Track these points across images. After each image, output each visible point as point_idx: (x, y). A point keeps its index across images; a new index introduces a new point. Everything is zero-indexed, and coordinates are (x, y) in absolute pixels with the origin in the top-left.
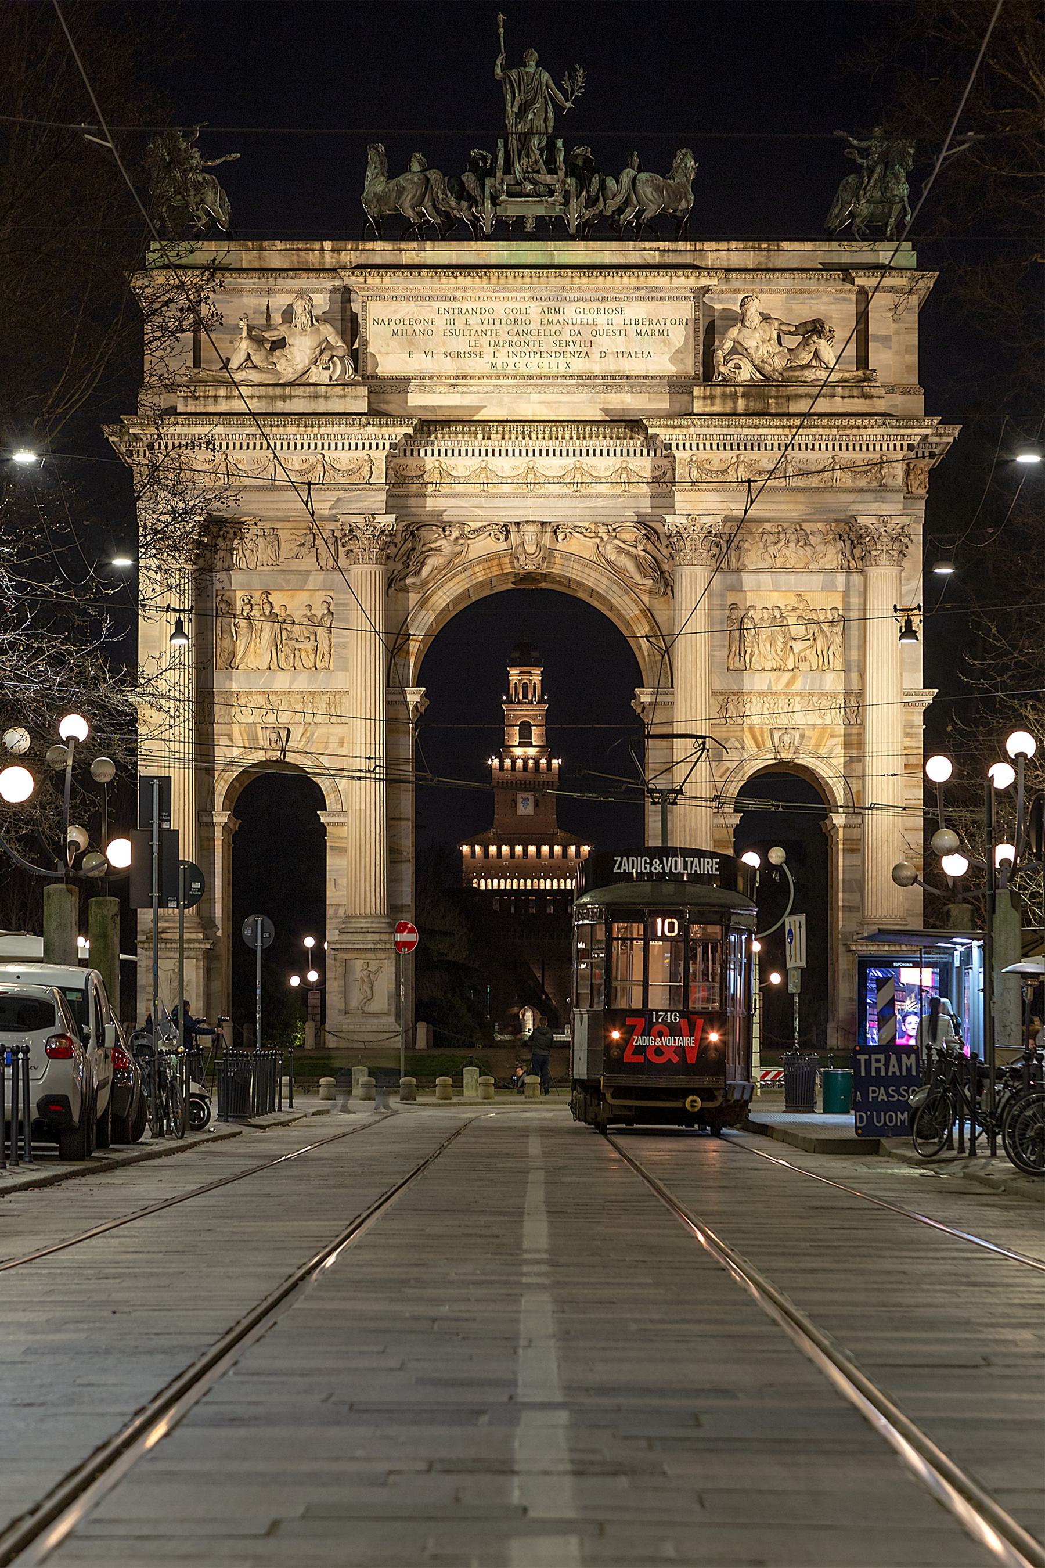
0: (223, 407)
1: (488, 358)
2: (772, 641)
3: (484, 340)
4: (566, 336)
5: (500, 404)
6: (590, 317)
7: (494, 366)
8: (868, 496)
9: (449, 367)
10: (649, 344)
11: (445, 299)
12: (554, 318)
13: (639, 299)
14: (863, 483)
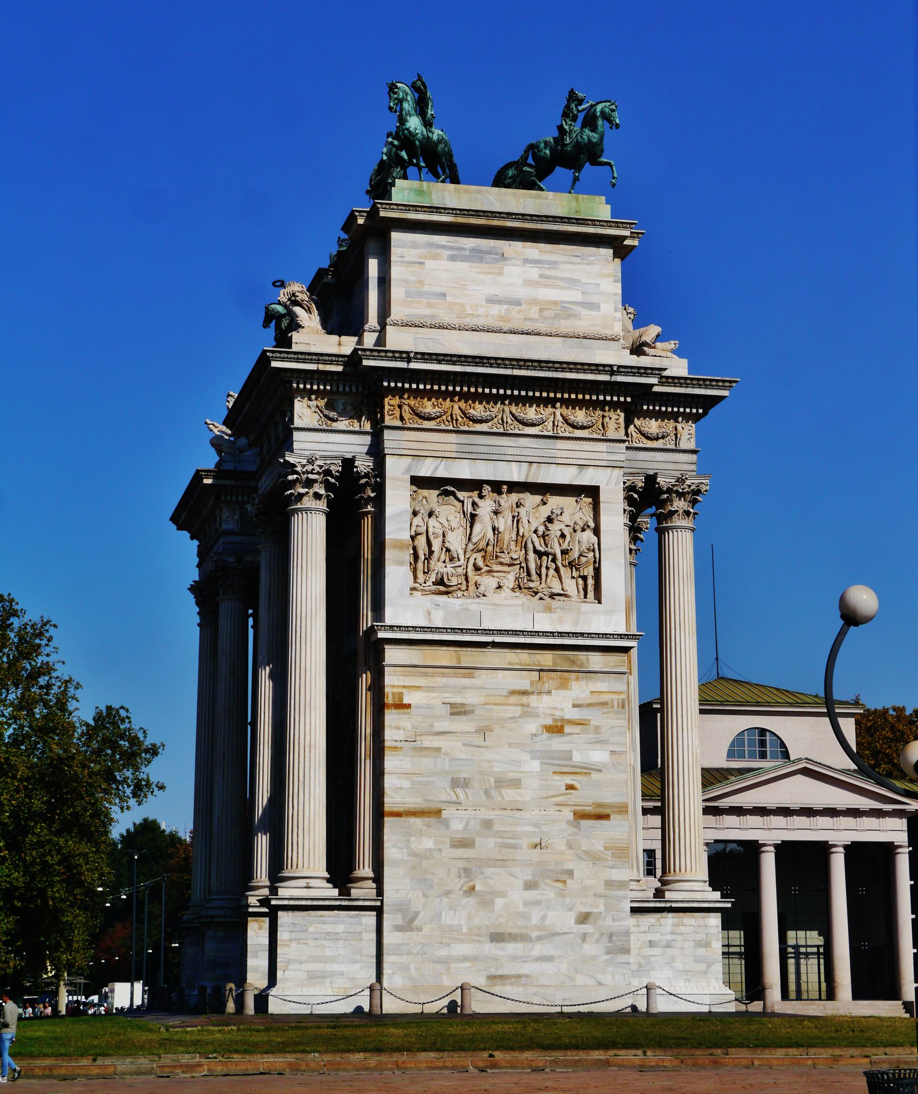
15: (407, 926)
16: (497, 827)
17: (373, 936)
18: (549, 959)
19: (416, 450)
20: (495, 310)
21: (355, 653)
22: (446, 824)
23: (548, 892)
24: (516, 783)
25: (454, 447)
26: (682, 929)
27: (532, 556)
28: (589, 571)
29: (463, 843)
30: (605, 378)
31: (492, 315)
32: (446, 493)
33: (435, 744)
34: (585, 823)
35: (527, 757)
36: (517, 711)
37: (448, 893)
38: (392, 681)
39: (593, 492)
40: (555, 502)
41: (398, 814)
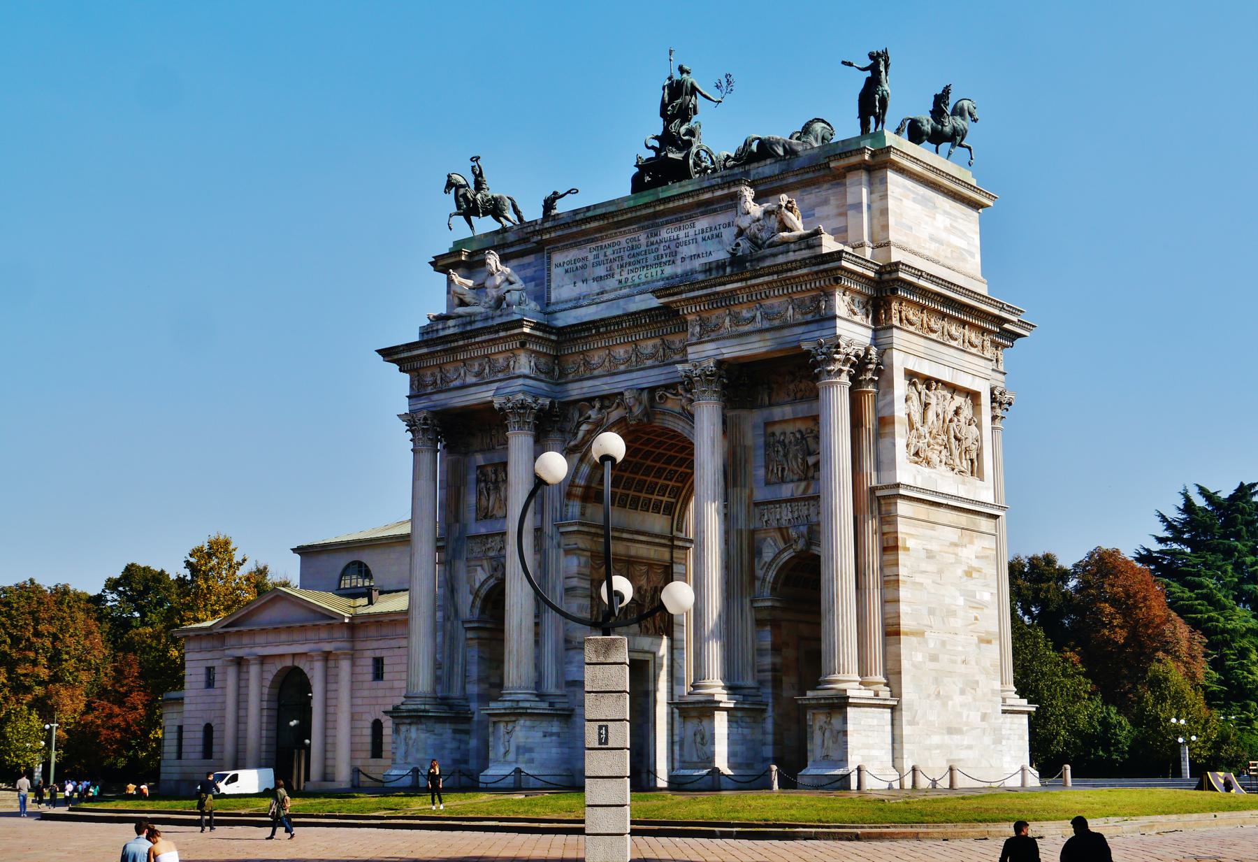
0: (442, 333)
1: (617, 277)
2: (796, 457)
3: (615, 265)
4: (661, 251)
5: (618, 307)
6: (675, 234)
7: (620, 282)
8: (812, 327)
9: (595, 287)
10: (710, 246)
11: (593, 241)
12: (654, 239)
13: (704, 214)
14: (809, 317)
15: (910, 723)
16: (948, 647)
17: (889, 728)
18: (970, 747)
19: (910, 351)
20: (934, 246)
21: (878, 503)
22: (926, 642)
23: (968, 698)
24: (952, 613)
25: (922, 349)
26: (1015, 726)
27: (953, 440)
28: (974, 456)
29: (934, 658)
30: (996, 312)
31: (930, 249)
32: (914, 384)
33: (921, 580)
34: (984, 646)
35: (958, 594)
36: (951, 559)
37: (929, 696)
38: (903, 528)
39: (974, 396)
40: (959, 400)
41: (906, 634)
